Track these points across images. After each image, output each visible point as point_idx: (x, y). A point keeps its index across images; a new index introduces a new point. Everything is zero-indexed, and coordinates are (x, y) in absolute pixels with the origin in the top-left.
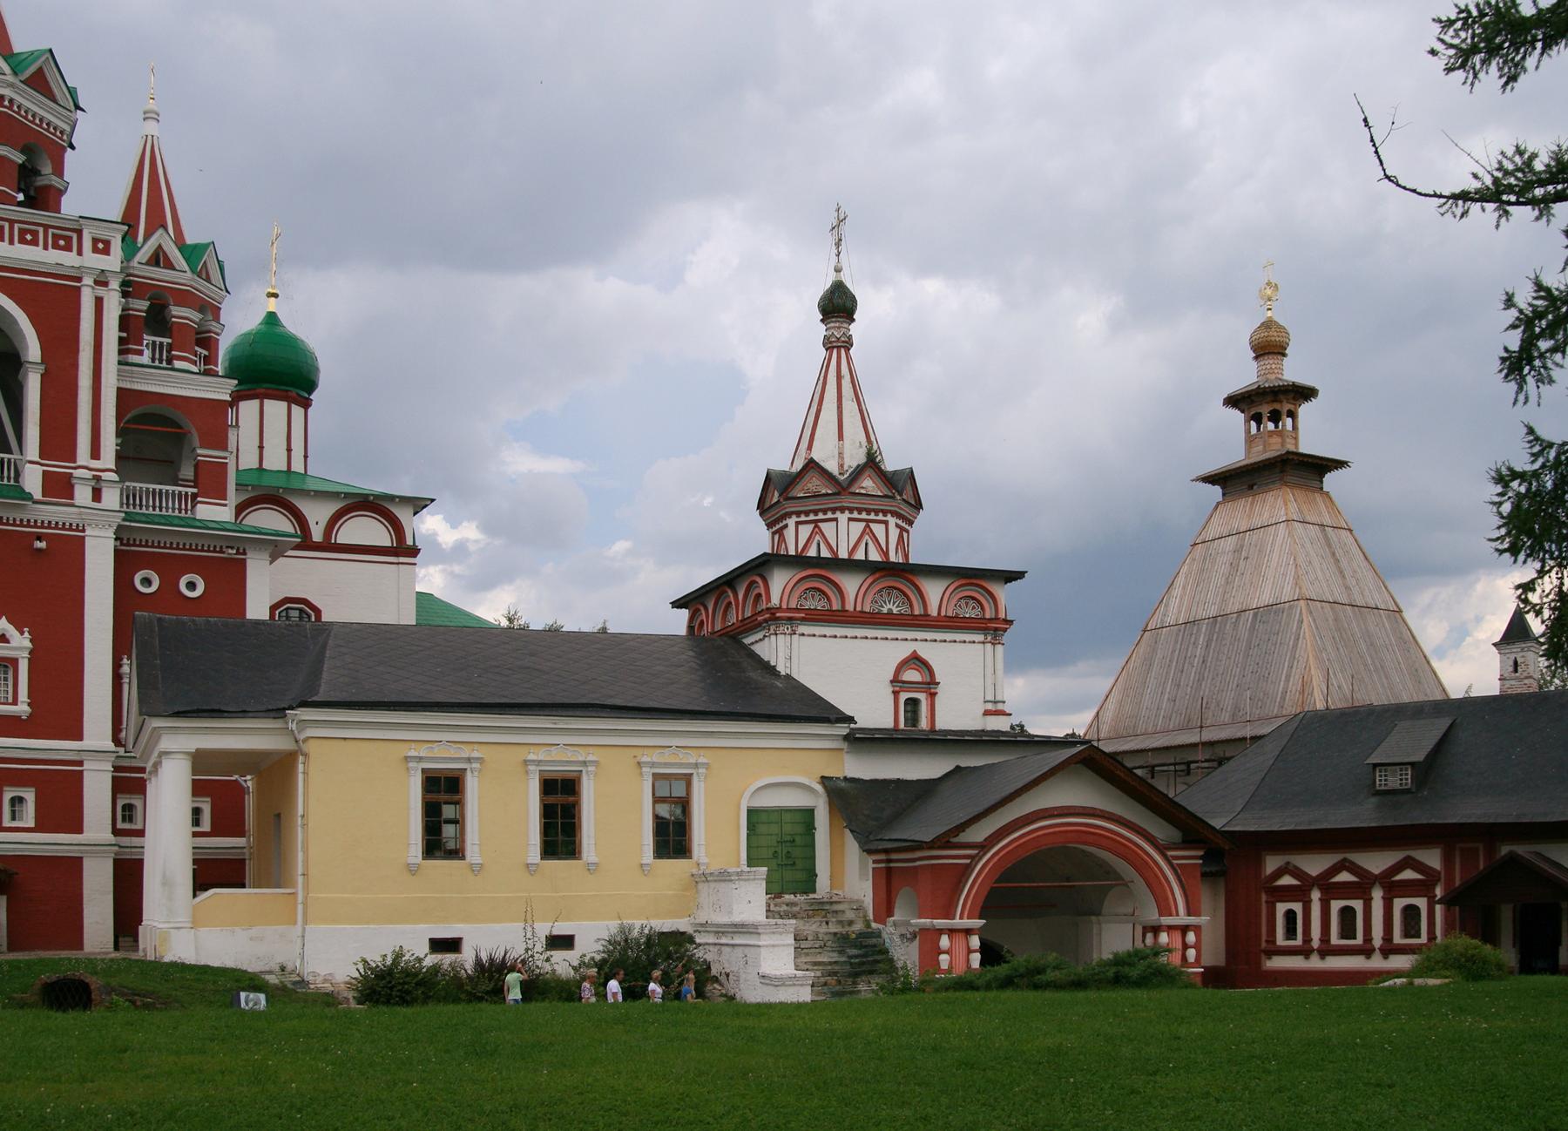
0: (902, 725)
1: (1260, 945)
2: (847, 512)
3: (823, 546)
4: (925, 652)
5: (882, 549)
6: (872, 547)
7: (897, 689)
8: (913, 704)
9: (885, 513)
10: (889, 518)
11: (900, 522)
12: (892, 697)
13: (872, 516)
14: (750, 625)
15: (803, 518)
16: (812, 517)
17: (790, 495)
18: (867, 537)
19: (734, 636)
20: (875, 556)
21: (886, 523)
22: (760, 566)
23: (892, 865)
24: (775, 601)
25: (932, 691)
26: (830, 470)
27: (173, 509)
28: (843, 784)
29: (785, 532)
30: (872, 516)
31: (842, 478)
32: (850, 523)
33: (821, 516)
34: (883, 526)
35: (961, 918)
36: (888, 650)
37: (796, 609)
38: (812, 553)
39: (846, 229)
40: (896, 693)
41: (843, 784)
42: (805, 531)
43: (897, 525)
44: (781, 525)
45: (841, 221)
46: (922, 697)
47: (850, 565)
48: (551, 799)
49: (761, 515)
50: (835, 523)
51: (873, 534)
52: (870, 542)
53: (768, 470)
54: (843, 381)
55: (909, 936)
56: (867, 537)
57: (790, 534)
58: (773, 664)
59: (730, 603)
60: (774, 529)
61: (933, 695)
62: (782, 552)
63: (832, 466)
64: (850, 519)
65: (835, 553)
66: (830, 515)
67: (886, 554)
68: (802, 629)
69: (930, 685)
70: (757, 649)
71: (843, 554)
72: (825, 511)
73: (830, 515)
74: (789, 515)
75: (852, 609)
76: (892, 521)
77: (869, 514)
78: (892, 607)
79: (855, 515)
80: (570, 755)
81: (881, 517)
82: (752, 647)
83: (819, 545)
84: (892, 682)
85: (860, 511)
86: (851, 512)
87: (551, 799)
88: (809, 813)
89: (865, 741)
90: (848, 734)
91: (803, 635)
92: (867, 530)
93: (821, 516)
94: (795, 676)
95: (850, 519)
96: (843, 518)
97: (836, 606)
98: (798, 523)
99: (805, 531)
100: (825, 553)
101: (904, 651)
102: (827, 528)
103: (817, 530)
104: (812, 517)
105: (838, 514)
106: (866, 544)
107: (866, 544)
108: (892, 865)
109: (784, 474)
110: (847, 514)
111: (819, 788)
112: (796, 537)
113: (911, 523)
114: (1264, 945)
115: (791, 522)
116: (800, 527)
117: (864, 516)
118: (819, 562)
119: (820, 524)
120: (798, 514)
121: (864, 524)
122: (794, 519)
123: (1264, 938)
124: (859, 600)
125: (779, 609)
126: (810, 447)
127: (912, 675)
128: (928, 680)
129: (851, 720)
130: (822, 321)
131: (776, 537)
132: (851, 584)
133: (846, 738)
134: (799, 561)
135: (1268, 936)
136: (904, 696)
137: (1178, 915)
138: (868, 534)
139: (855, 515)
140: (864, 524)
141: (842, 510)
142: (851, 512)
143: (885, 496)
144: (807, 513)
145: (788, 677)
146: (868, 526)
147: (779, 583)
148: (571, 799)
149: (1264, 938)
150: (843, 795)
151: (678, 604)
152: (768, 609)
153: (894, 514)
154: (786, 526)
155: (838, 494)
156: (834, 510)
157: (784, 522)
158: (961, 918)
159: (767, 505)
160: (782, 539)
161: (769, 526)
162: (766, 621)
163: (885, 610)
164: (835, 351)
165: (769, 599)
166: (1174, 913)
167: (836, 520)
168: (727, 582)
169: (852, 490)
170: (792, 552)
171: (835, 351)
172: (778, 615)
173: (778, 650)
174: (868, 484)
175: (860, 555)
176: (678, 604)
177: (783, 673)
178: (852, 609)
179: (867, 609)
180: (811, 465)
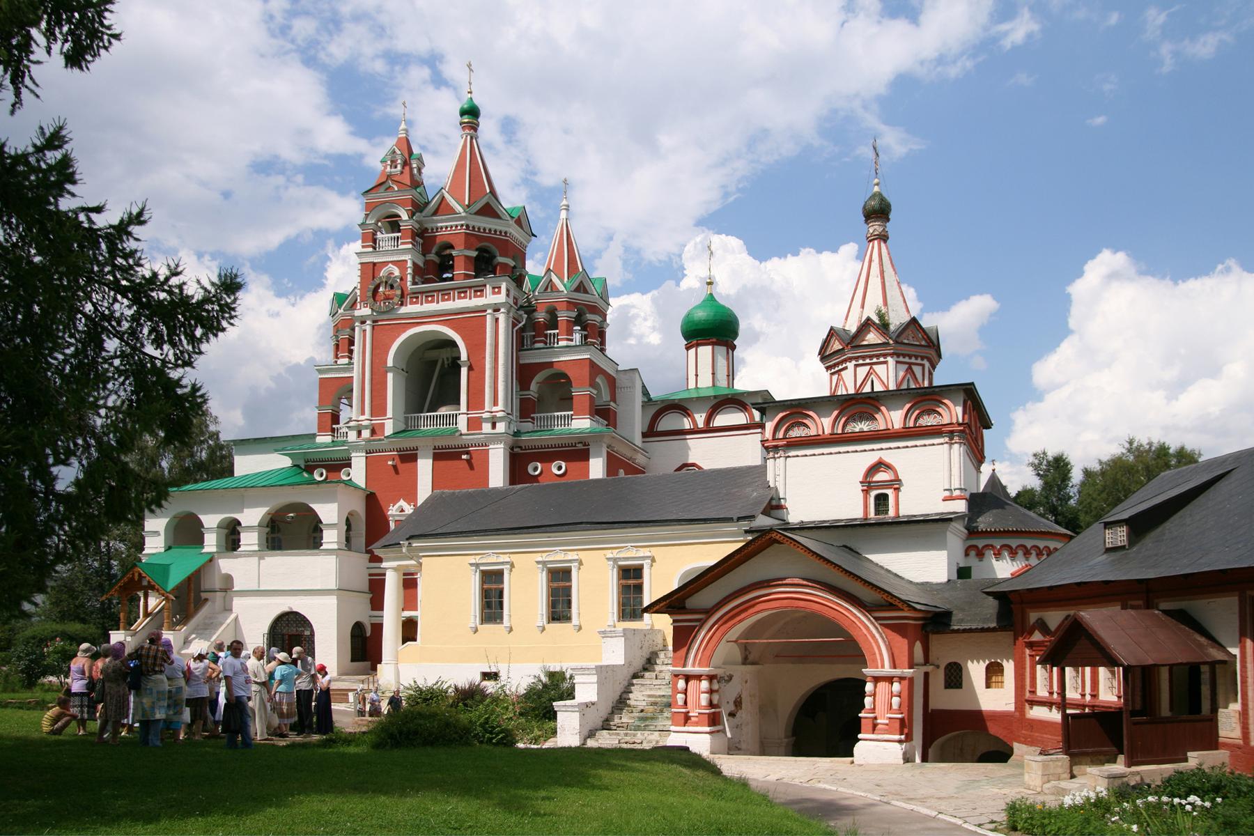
1: (1024, 695)
4: (888, 457)
5: (883, 383)
7: (865, 488)
8: (882, 500)
9: (885, 356)
10: (889, 359)
12: (861, 495)
13: (875, 360)
27: (541, 426)
30: (875, 360)
34: (884, 366)
35: (693, 665)
36: (858, 460)
40: (866, 492)
46: (890, 492)
54: (873, 264)
55: (726, 678)
56: (872, 376)
61: (897, 490)
64: (856, 366)
66: (844, 365)
69: (896, 484)
78: (863, 426)
79: (861, 362)
81: (882, 359)
84: (861, 482)
85: (864, 358)
91: (789, 457)
95: (856, 366)
101: (871, 458)
106: (872, 382)
110: (854, 362)
114: (1028, 695)
117: (868, 361)
123: (1028, 688)
127: (881, 476)
128: (893, 478)
135: (1031, 687)
136: (874, 493)
137: (883, 666)
139: (861, 362)
140: (868, 367)
143: (884, 343)
149: (1028, 688)
153: (892, 355)
158: (693, 665)
166: (880, 665)
174: (872, 337)
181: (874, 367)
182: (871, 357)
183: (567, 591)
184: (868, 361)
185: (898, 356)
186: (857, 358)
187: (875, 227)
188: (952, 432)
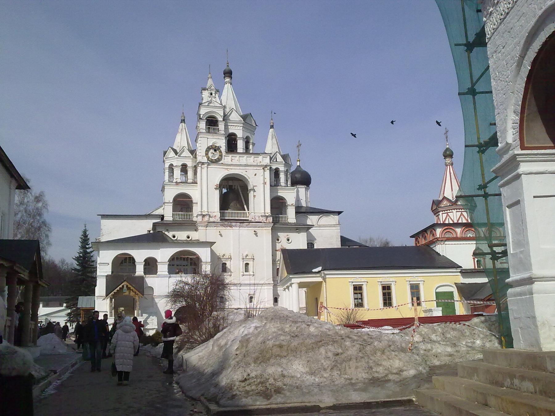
0: (476, 267)
3: (450, 219)
6: (463, 219)
12: (473, 260)
14: (433, 242)
15: (444, 212)
18: (462, 216)
19: (428, 245)
20: (464, 221)
22: (433, 227)
23: (476, 306)
24: (438, 236)
25: (484, 257)
26: (450, 199)
28: (461, 285)
29: (439, 216)
31: (453, 200)
32: (457, 213)
33: (448, 211)
37: (444, 238)
38: (447, 222)
39: (449, 134)
40: (474, 259)
41: (461, 285)
42: (445, 215)
45: (447, 132)
47: (457, 225)
48: (385, 291)
49: (432, 211)
52: (463, 217)
53: (433, 201)
54: (451, 174)
56: (462, 216)
57: (440, 216)
58: (439, 252)
59: (426, 236)
62: (439, 223)
63: (451, 198)
65: (453, 221)
66: (451, 211)
67: (468, 220)
68: (446, 243)
70: (434, 248)
71: (456, 222)
73: (451, 211)
74: (440, 212)
75: (459, 236)
77: (462, 210)
79: (458, 210)
80: (388, 280)
82: (433, 248)
87: (385, 291)
88: (452, 293)
89: (466, 273)
90: (461, 271)
92: (462, 214)
93: (448, 211)
94: (445, 255)
95: (457, 212)
96: (454, 211)
97: (455, 236)
98: (442, 214)
100: (451, 222)
103: (448, 215)
104: (446, 212)
105: (453, 211)
106: (462, 218)
107: (462, 218)
108: (476, 306)
109: (438, 200)
110: (456, 210)
111: (454, 286)
112: (442, 217)
113: (474, 211)
115: (441, 213)
116: (443, 215)
117: (460, 210)
118: (449, 225)
119: (449, 214)
120: (442, 211)
121: (460, 213)
122: (441, 212)
124: (461, 235)
125: (439, 238)
126: (444, 194)
129: (461, 267)
130: (444, 158)
131: (437, 218)
132: (459, 230)
133: (460, 272)
134: (444, 225)
139: (458, 210)
140: (460, 213)
141: (454, 209)
143: (466, 205)
144: (444, 211)
145: (443, 256)
146: (462, 213)
147: (439, 231)
148: (390, 291)
150: (461, 288)
151: (412, 237)
152: (436, 238)
154: (439, 215)
155: (453, 205)
159: (433, 209)
160: (439, 218)
162: (436, 241)
163: (468, 236)
164: (448, 166)
165: (436, 236)
167: (452, 212)
168: (425, 231)
170: (442, 222)
171: (448, 166)
172: (439, 239)
173: (440, 248)
175: (460, 221)
176: (412, 237)
177: (442, 255)
178: (459, 236)
179: (463, 236)
180: (444, 198)
183: (390, 294)
184: (460, 210)
186: (457, 209)
187: (448, 160)
188: (500, 239)
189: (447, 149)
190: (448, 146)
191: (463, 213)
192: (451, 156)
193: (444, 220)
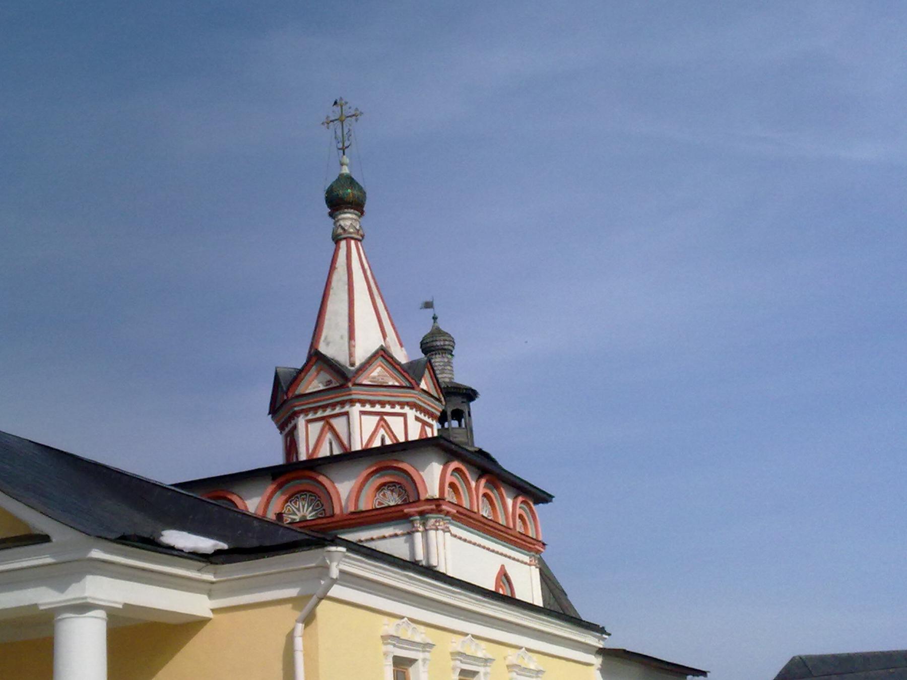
2: (358, 405)
9: (402, 404)
10: (407, 410)
11: (418, 414)
13: (388, 409)
16: (320, 414)
17: (297, 392)
18: (382, 432)
21: (404, 415)
30: (388, 409)
32: (363, 417)
34: (401, 419)
42: (315, 428)
43: (417, 419)
44: (290, 426)
50: (343, 420)
51: (390, 429)
53: (276, 368)
56: (382, 432)
60: (287, 430)
66: (338, 410)
72: (333, 406)
76: (411, 413)
79: (368, 408)
81: (397, 409)
83: (331, 444)
85: (373, 403)
86: (363, 405)
95: (363, 413)
99: (315, 428)
102: (339, 424)
105: (347, 408)
110: (358, 407)
116: (311, 426)
117: (378, 408)
121: (378, 418)
138: (382, 426)
140: (378, 418)
141: (352, 402)
142: (363, 405)
146: (382, 419)
153: (413, 405)
156: (342, 404)
157: (293, 422)
161: (281, 428)
169: (359, 381)
181: (386, 417)
182: (383, 404)
184: (378, 408)
185: (416, 411)
186: (363, 402)
189: (348, 181)
190: (346, 170)
191: (386, 417)
192: (358, 206)
193: (310, 451)
